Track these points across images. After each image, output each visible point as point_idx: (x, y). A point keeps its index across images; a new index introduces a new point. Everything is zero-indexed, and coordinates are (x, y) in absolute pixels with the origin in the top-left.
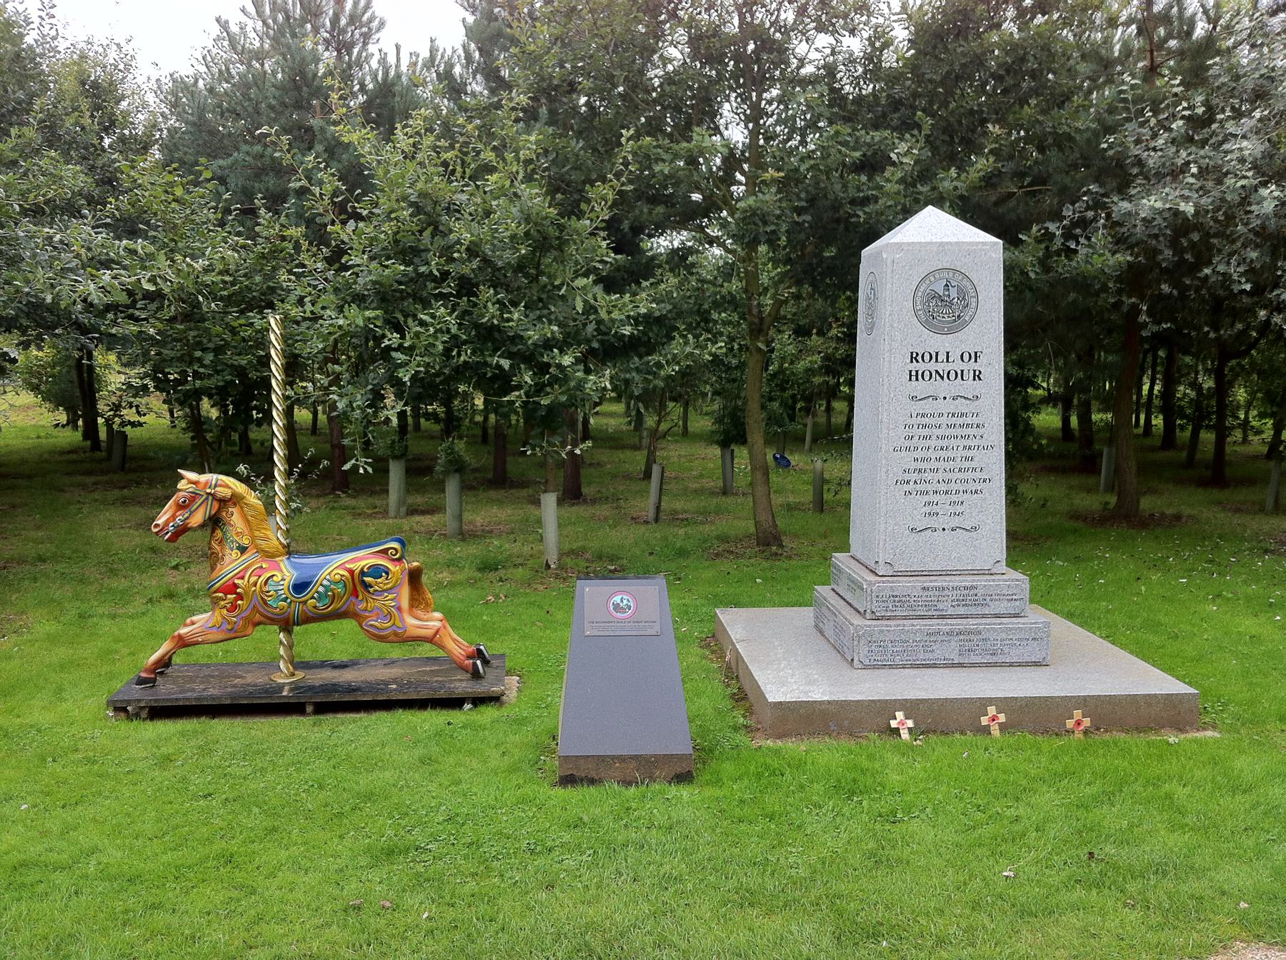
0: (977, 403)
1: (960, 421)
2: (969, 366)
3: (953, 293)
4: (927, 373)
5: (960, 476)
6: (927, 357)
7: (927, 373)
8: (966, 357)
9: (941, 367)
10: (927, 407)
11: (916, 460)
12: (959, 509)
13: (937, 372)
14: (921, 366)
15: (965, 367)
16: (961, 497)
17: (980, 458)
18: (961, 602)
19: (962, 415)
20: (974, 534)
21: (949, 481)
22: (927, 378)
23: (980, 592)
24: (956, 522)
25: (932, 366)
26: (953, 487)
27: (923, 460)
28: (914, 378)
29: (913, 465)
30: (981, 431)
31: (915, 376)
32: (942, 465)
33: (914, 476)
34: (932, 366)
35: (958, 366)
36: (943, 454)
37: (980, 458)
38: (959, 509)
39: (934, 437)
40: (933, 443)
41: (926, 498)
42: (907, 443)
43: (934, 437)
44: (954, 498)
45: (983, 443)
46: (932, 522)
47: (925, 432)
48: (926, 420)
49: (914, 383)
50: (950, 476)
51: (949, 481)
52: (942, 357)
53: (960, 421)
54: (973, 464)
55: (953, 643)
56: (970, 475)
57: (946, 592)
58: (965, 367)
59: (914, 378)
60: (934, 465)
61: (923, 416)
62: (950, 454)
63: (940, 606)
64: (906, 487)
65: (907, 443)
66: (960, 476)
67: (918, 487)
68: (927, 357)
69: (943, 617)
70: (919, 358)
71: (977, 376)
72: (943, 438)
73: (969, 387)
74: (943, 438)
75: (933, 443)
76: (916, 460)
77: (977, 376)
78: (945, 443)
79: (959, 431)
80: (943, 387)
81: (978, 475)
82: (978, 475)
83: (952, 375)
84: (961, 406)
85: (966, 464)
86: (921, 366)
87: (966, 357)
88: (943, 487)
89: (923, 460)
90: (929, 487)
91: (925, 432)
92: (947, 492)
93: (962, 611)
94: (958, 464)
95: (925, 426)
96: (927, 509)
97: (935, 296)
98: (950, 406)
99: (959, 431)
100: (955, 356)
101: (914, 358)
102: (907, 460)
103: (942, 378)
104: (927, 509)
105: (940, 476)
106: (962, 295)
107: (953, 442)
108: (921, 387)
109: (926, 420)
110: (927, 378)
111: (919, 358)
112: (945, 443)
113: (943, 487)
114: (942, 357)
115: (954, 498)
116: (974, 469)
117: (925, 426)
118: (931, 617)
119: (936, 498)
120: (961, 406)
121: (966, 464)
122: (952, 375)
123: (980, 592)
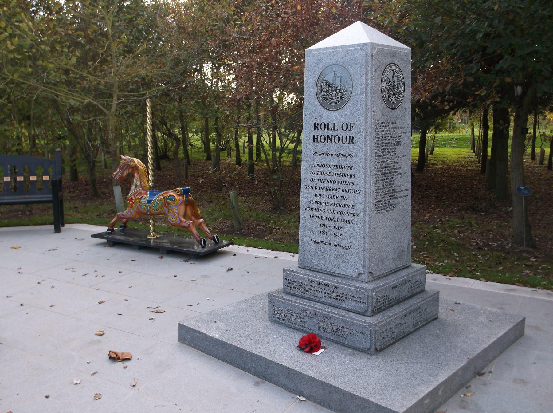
0: (350, 159)
1: (341, 171)
4: (323, 137)
7: (323, 137)
8: (345, 126)
9: (331, 133)
11: (316, 195)
12: (339, 232)
14: (319, 133)
17: (353, 199)
18: (329, 295)
21: (334, 212)
23: (341, 291)
24: (336, 240)
25: (326, 133)
26: (337, 216)
27: (320, 196)
28: (316, 140)
30: (353, 180)
31: (316, 139)
32: (329, 200)
33: (315, 206)
34: (326, 133)
35: (340, 133)
36: (331, 193)
37: (353, 199)
38: (339, 232)
39: (326, 181)
40: (325, 185)
41: (321, 222)
42: (312, 184)
43: (326, 181)
44: (337, 224)
46: (323, 238)
47: (321, 177)
48: (322, 169)
49: (316, 144)
50: (334, 208)
51: (334, 212)
52: (331, 127)
53: (341, 171)
54: (348, 202)
55: (315, 320)
56: (345, 210)
57: (321, 286)
59: (316, 140)
61: (320, 166)
62: (335, 193)
63: (319, 294)
64: (311, 213)
69: (319, 302)
70: (319, 127)
71: (351, 140)
72: (331, 182)
73: (346, 148)
74: (331, 182)
75: (325, 185)
76: (316, 195)
78: (331, 186)
79: (340, 179)
80: (332, 148)
81: (350, 210)
82: (350, 210)
84: (341, 161)
85: (343, 202)
86: (319, 133)
87: (345, 126)
89: (320, 196)
90: (323, 215)
91: (321, 177)
93: (330, 301)
96: (321, 229)
98: (332, 161)
99: (340, 179)
103: (331, 141)
104: (321, 229)
105: (329, 207)
107: (337, 186)
109: (322, 169)
111: (319, 127)
112: (331, 186)
113: (330, 216)
114: (331, 127)
115: (337, 224)
116: (348, 206)
118: (313, 300)
119: (327, 222)
120: (341, 161)
121: (343, 202)
123: (341, 291)
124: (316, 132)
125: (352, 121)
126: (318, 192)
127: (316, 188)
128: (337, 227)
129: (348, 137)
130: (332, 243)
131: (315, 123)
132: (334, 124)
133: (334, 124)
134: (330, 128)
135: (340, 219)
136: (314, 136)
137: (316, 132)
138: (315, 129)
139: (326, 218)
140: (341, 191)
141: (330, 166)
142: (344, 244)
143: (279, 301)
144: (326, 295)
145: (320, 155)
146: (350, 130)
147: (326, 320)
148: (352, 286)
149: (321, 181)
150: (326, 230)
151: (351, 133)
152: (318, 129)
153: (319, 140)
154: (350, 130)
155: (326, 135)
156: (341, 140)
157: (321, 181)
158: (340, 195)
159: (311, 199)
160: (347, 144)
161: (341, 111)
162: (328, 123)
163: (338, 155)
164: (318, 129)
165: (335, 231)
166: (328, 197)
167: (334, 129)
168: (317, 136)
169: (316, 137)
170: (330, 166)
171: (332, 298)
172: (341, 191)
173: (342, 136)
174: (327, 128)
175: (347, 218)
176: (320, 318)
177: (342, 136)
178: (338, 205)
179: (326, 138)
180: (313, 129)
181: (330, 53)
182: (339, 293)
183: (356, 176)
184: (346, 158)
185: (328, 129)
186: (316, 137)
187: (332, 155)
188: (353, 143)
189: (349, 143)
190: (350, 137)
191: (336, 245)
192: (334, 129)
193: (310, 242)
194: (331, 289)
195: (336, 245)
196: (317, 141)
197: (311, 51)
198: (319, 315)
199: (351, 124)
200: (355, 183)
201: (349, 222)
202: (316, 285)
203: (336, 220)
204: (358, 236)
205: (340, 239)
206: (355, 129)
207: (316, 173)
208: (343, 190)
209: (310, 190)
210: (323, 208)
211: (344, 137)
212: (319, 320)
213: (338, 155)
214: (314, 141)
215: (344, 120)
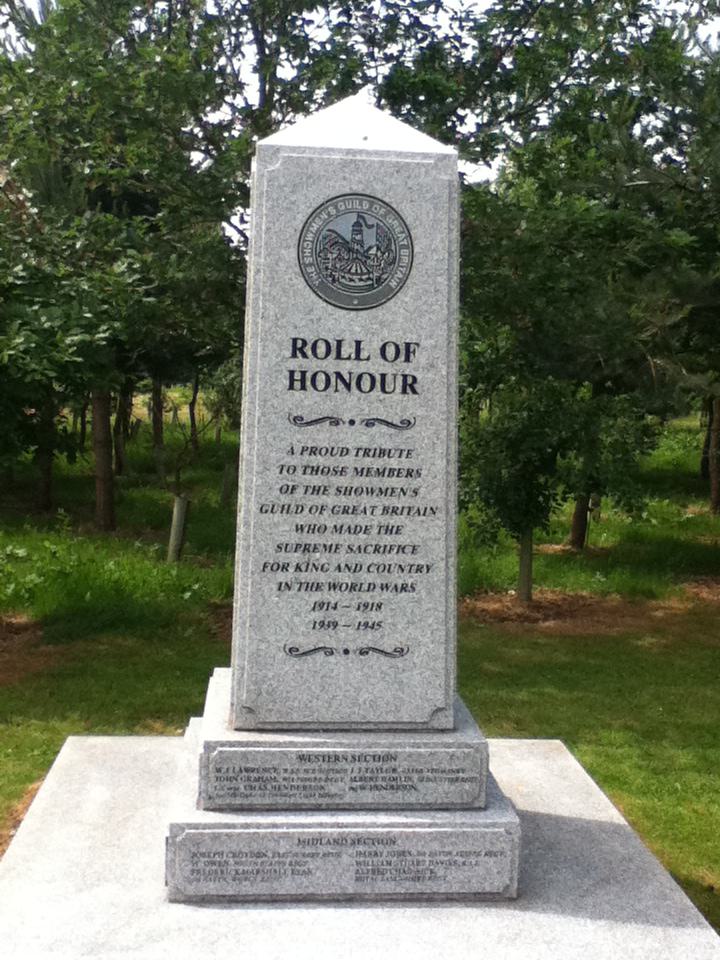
0: (408, 433)
2: (394, 369)
3: (370, 238)
4: (321, 378)
5: (377, 559)
6: (321, 349)
7: (321, 378)
8: (391, 351)
9: (345, 367)
10: (322, 436)
11: (300, 528)
12: (374, 616)
13: (339, 375)
14: (311, 365)
15: (388, 369)
16: (378, 596)
17: (413, 530)
18: (365, 782)
19: (383, 453)
20: (399, 662)
21: (358, 568)
22: (321, 385)
23: (402, 765)
24: (368, 638)
25: (331, 365)
26: (365, 578)
27: (312, 529)
28: (297, 385)
29: (294, 538)
30: (415, 483)
31: (298, 381)
32: (345, 539)
33: (295, 558)
34: (331, 365)
35: (377, 367)
36: (347, 520)
37: (413, 530)
38: (374, 616)
39: (332, 491)
40: (330, 500)
41: (317, 597)
42: (285, 499)
43: (332, 491)
44: (366, 597)
45: (418, 503)
46: (327, 639)
47: (316, 480)
48: (318, 460)
49: (298, 394)
50: (359, 558)
51: (358, 568)
52: (348, 350)
54: (401, 540)
55: (345, 859)
56: (392, 558)
57: (342, 765)
58: (388, 369)
59: (297, 385)
60: (331, 538)
61: (314, 451)
62: (361, 520)
63: (333, 789)
64: (281, 577)
65: (285, 499)
66: (377, 559)
67: (304, 576)
68: (321, 349)
70: (308, 350)
71: (409, 385)
72: (348, 491)
73: (396, 405)
74: (348, 491)
75: (330, 500)
77: (409, 385)
78: (350, 501)
79: (376, 482)
80: (349, 404)
81: (407, 559)
82: (407, 559)
83: (366, 384)
84: (381, 437)
85: (388, 540)
86: (311, 365)
87: (391, 351)
88: (346, 578)
89: (312, 529)
90: (322, 578)
91: (316, 480)
92: (353, 587)
93: (368, 797)
94: (374, 538)
95: (315, 470)
96: (318, 615)
97: (336, 241)
98: (360, 437)
99: (376, 482)
100: (371, 348)
101: (298, 348)
102: (284, 529)
103: (348, 386)
104: (318, 615)
105: (342, 557)
106: (386, 241)
107: (366, 501)
108: (310, 402)
109: (318, 460)
110: (321, 385)
112: (350, 501)
113: (346, 578)
114: (348, 350)
115: (366, 597)
116: (402, 549)
117: (315, 470)
119: (333, 597)
120: (381, 437)
121: (388, 540)
122: (366, 384)
123: (402, 765)
124: (298, 364)
125: (411, 338)
126: (303, 519)
127: (300, 509)
128: (366, 606)
129: (400, 380)
130: (351, 647)
131: (295, 340)
132: (358, 343)
133: (358, 343)
134: (344, 354)
135: (378, 582)
136: (292, 373)
137: (298, 364)
138: (294, 355)
139: (333, 586)
140: (378, 511)
141: (345, 451)
142: (388, 645)
143: (216, 837)
144: (354, 784)
145: (309, 424)
146: (407, 359)
147: (380, 848)
148: (436, 745)
149: (316, 490)
150: (334, 615)
151: (409, 369)
152: (305, 355)
153: (308, 383)
154: (407, 359)
155: (331, 371)
156: (378, 384)
157: (316, 490)
158: (375, 523)
159: (283, 540)
160: (397, 396)
161: (379, 312)
162: (339, 343)
163: (369, 423)
164: (305, 355)
165: (360, 617)
166: (338, 529)
167: (358, 357)
168: (303, 373)
169: (297, 376)
170: (345, 451)
171: (376, 787)
172: (378, 511)
173: (383, 376)
174: (333, 354)
175: (397, 578)
176: (361, 848)
177: (383, 376)
178: (370, 549)
179: (333, 379)
180: (288, 353)
181: (344, 164)
182: (400, 770)
183: (424, 472)
184: (392, 431)
185: (339, 356)
186: (297, 376)
187: (352, 422)
188: (414, 392)
189: (404, 391)
190: (405, 377)
191: (363, 652)
192: (358, 357)
193: (282, 654)
194: (373, 765)
195: (363, 652)
196: (303, 387)
197: (277, 150)
198: (358, 840)
199: (408, 345)
200: (422, 491)
201: (404, 588)
202: (325, 766)
203: (365, 587)
204: (430, 621)
205: (378, 634)
206: (420, 358)
207: (300, 471)
208: (385, 510)
209: (277, 517)
210: (324, 561)
211: (389, 379)
212: (360, 854)
213: (369, 423)
214: (291, 387)
215: (387, 335)
